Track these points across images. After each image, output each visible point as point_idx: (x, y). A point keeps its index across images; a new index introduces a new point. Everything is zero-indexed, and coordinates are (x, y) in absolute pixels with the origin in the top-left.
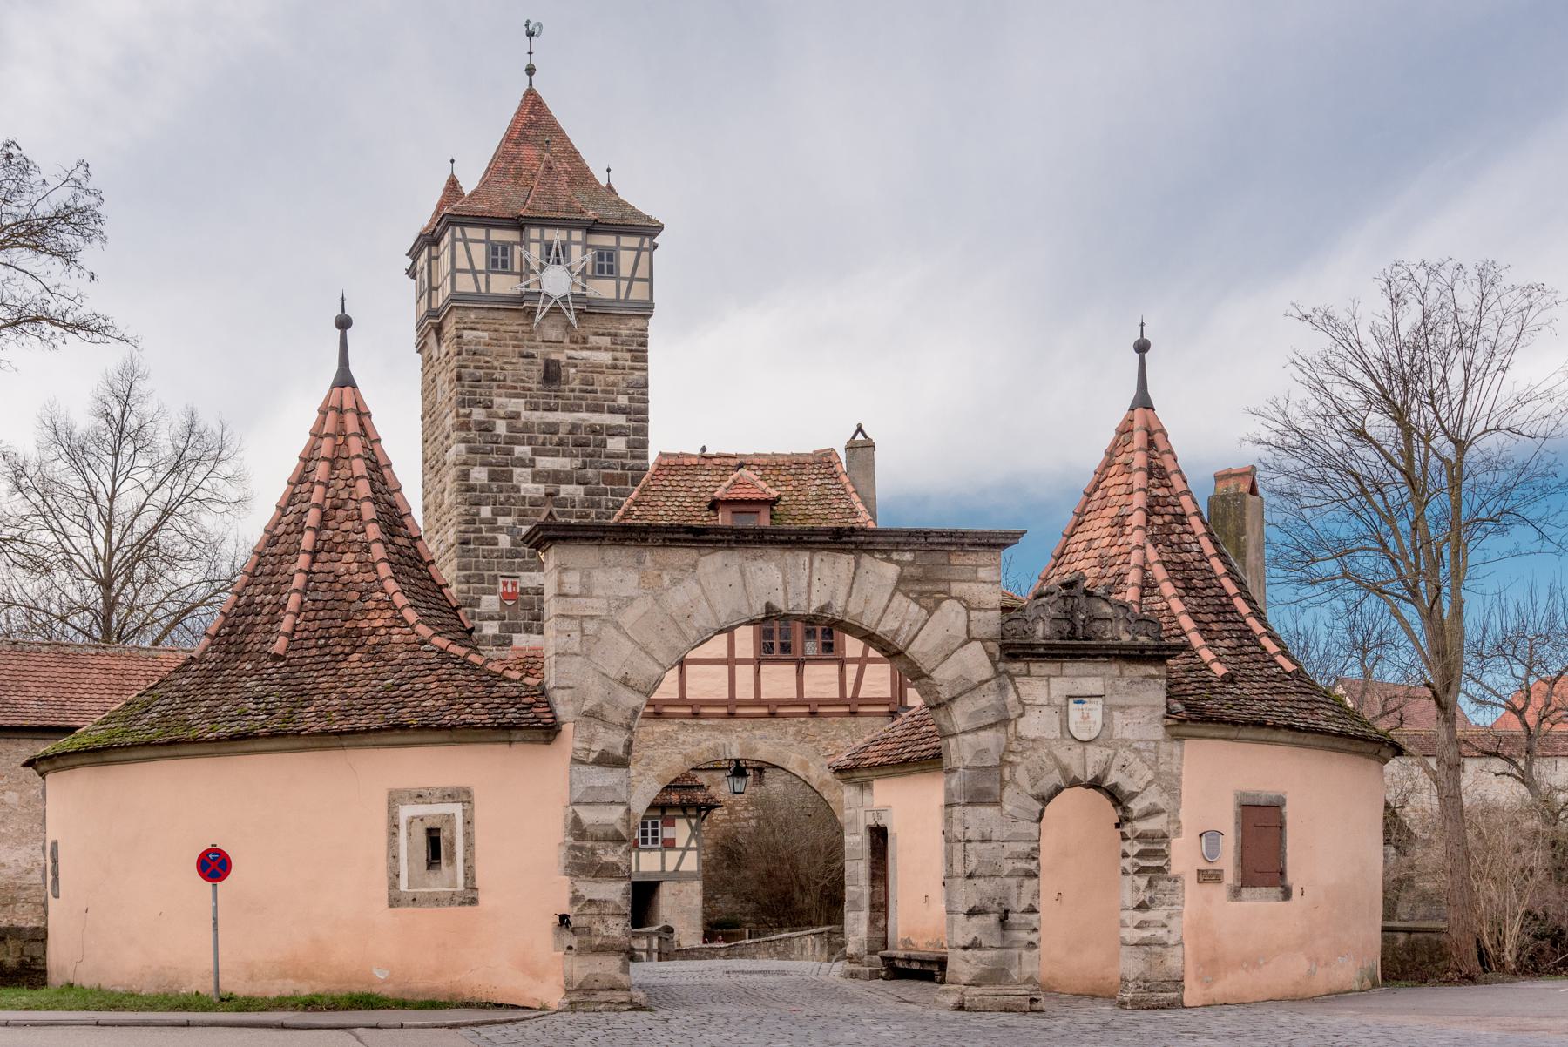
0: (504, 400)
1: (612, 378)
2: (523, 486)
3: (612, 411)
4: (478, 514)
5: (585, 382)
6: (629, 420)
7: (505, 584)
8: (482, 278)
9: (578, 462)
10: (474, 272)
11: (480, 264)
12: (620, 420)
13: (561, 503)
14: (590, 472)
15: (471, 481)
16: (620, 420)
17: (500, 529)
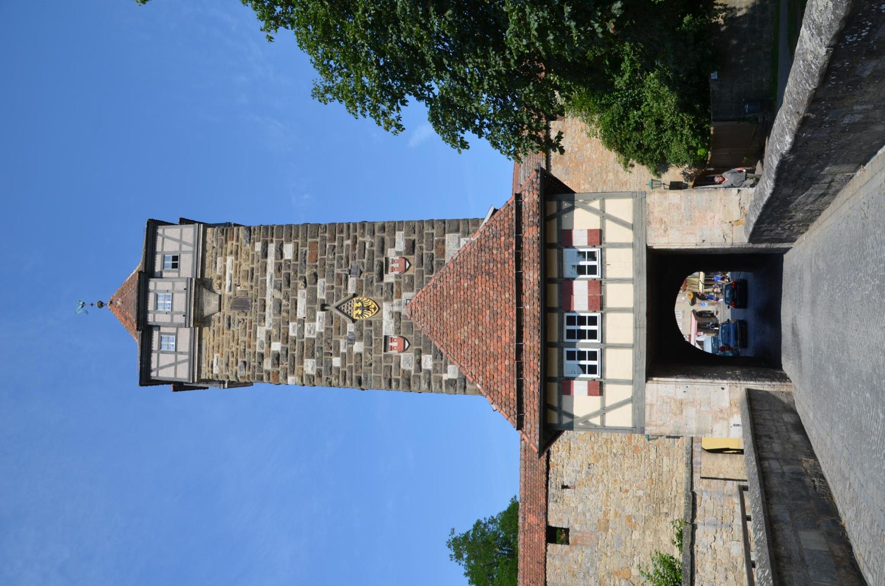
0: (257, 343)
1: (244, 256)
2: (317, 330)
3: (265, 255)
4: (338, 369)
5: (246, 278)
6: (272, 241)
7: (392, 348)
8: (181, 358)
9: (301, 283)
10: (176, 364)
11: (171, 358)
12: (272, 248)
13: (330, 297)
14: (307, 274)
15: (314, 373)
16: (272, 248)
17: (350, 350)
